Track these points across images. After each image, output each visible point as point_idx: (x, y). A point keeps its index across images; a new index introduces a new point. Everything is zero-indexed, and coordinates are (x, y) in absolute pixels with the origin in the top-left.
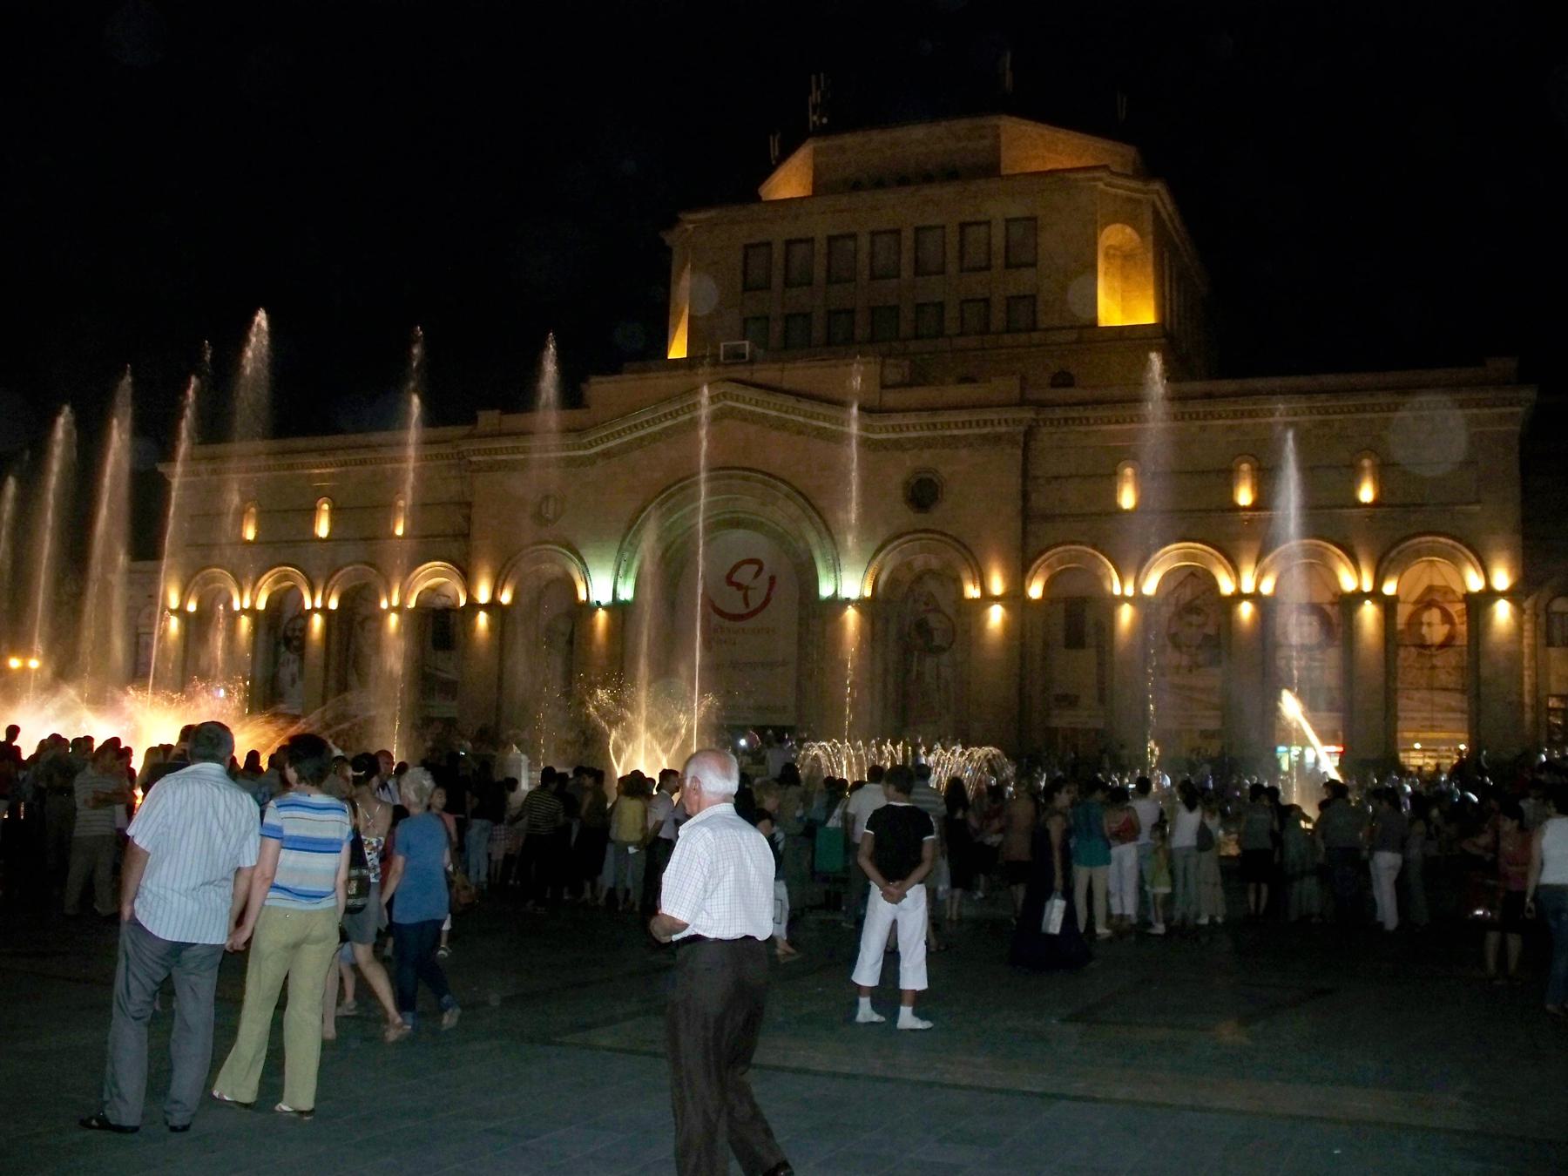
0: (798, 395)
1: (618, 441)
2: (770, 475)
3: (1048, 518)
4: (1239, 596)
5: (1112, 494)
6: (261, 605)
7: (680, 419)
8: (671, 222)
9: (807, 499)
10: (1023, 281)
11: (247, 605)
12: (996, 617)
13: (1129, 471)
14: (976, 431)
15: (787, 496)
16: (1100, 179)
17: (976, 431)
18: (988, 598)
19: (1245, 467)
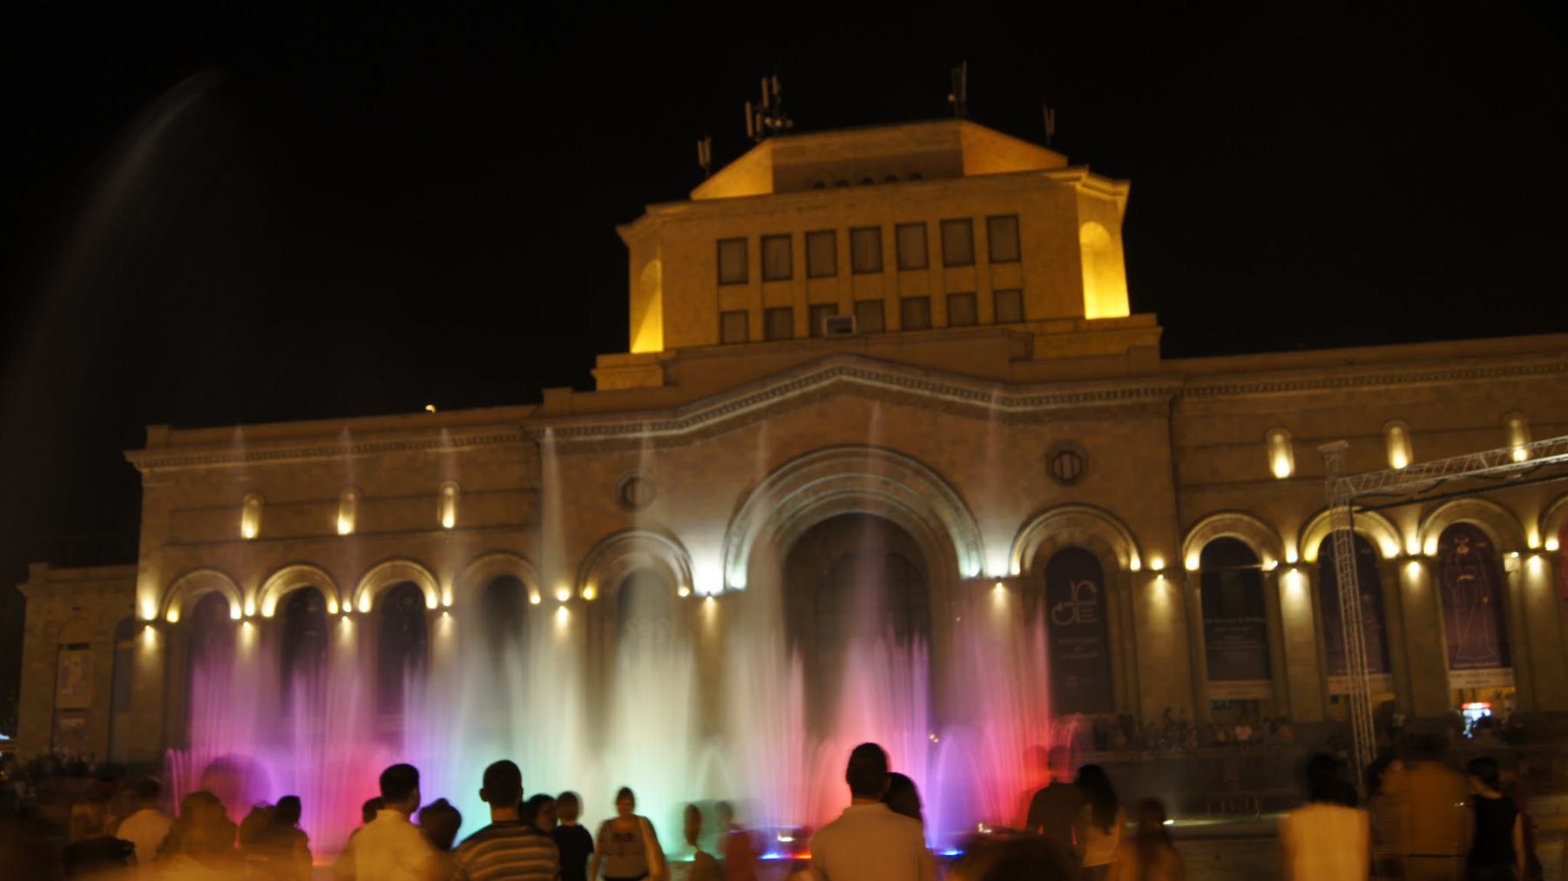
0: (928, 370)
1: (717, 419)
2: (900, 453)
4: (1405, 558)
5: (1266, 463)
6: (269, 610)
7: (790, 395)
8: (634, 213)
9: (938, 474)
10: (1007, 276)
11: (250, 610)
12: (1160, 590)
13: (1278, 439)
14: (1119, 402)
15: (918, 472)
16: (1078, 179)
17: (1119, 402)
19: (1396, 431)
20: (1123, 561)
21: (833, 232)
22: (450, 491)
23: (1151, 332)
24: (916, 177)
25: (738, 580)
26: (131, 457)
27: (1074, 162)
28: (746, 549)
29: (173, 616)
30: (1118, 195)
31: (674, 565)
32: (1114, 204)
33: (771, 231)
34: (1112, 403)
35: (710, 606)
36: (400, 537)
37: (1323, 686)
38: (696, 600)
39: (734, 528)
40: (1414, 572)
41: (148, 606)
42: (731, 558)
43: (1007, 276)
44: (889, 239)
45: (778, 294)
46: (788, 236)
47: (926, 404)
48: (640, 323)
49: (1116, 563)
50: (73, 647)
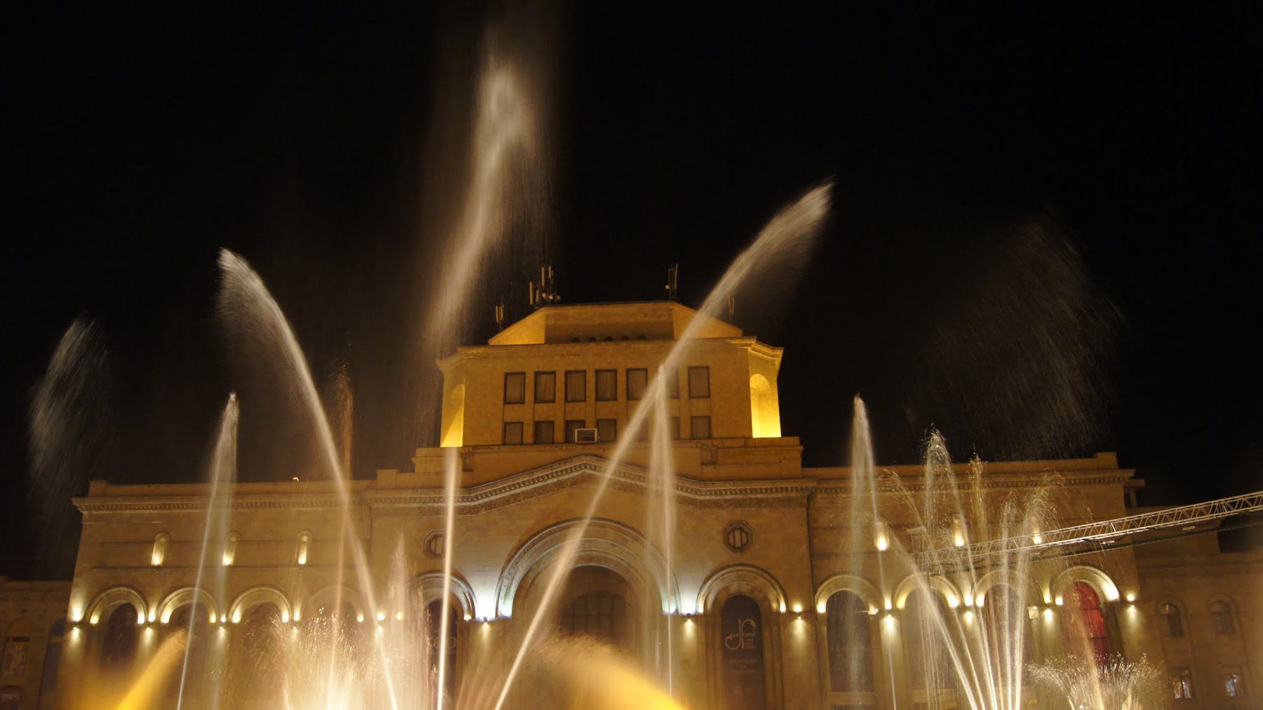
4: (962, 608)
7: (549, 481)
11: (152, 618)
14: (774, 495)
17: (774, 495)
18: (791, 615)
20: (774, 606)
22: (305, 539)
24: (642, 338)
25: (507, 610)
26: (76, 502)
27: (747, 334)
29: (94, 620)
30: (775, 356)
32: (773, 363)
33: (541, 369)
34: (770, 496)
35: (486, 629)
38: (475, 623)
39: (506, 574)
41: (76, 612)
42: (502, 595)
44: (622, 378)
46: (554, 373)
48: (447, 429)
49: (770, 606)
50: (17, 640)
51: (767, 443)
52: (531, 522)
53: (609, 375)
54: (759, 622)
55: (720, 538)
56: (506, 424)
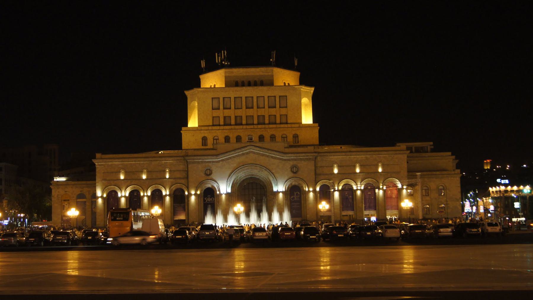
0: (268, 149)
3: (320, 174)
5: (333, 170)
6: (127, 195)
10: (283, 111)
11: (123, 195)
12: (311, 195)
18: (309, 191)
21: (241, 97)
23: (314, 136)
25: (229, 190)
26: (94, 161)
28: (231, 185)
29: (105, 195)
30: (312, 90)
31: (216, 187)
35: (224, 196)
36: (156, 178)
37: (341, 213)
38: (221, 195)
40: (359, 192)
41: (99, 193)
43: (283, 111)
44: (255, 100)
45: (227, 113)
47: (268, 156)
48: (190, 117)
50: (65, 200)
51: (308, 126)
52: (235, 165)
53: (250, 98)
54: (300, 192)
55: (289, 170)
56: (213, 117)
